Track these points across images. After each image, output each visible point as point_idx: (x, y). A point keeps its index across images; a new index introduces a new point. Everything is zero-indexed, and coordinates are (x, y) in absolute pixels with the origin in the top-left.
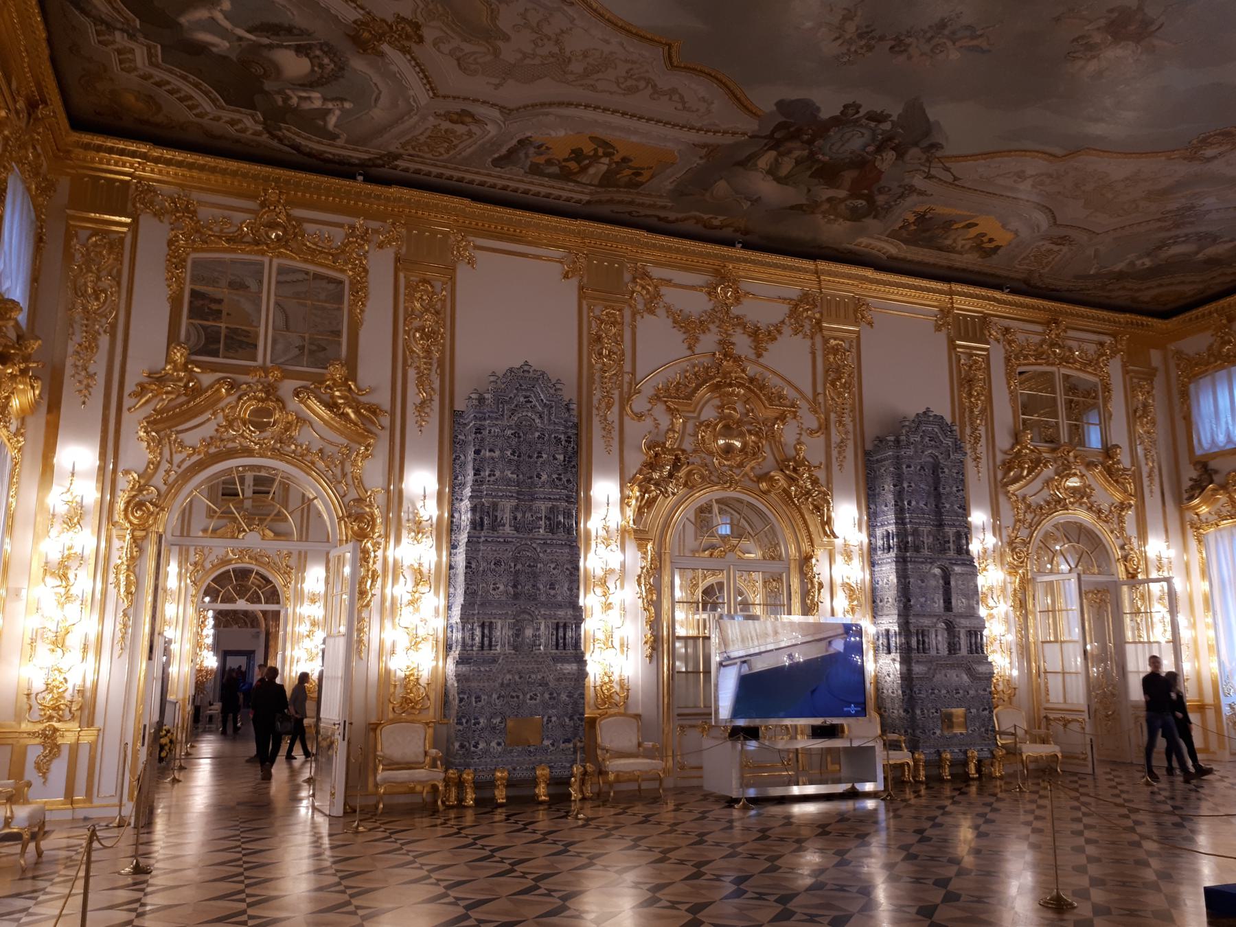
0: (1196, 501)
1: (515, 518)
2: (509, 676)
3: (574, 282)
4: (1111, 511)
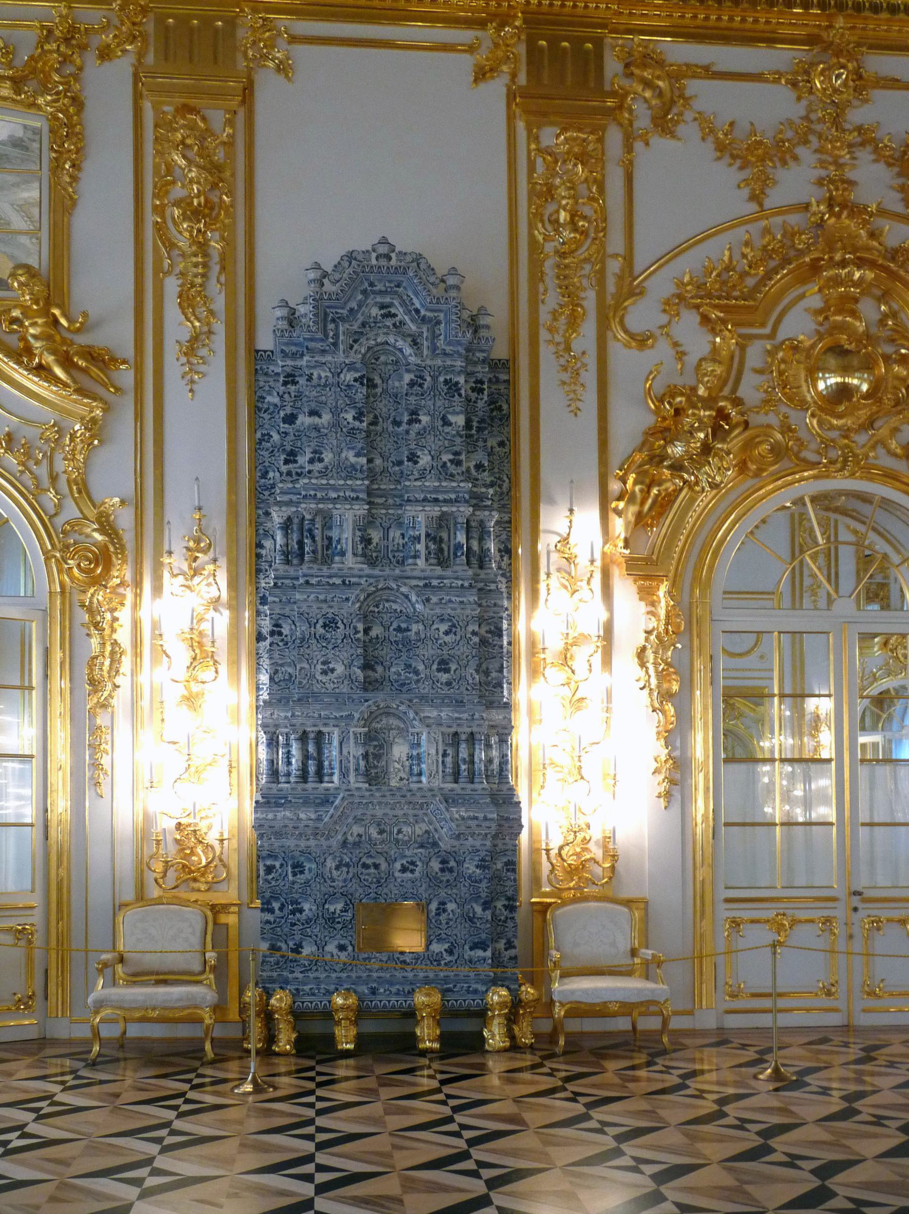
1: (367, 541)
2: (357, 829)
3: (497, 88)
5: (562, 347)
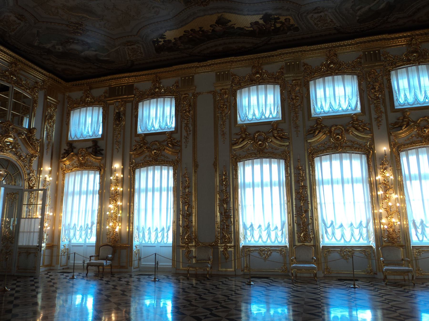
0: (65, 159)
4: (26, 157)
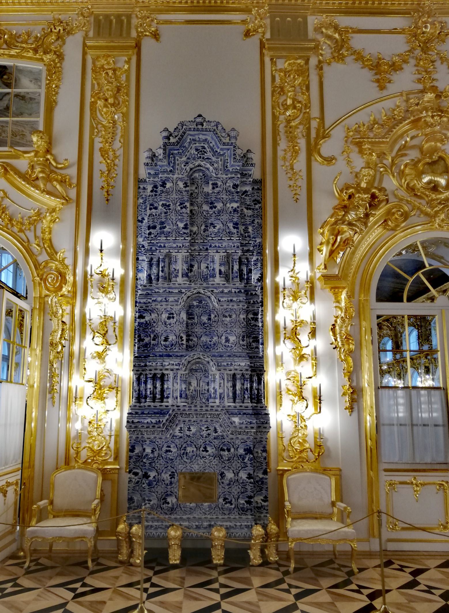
5: (289, 168)
